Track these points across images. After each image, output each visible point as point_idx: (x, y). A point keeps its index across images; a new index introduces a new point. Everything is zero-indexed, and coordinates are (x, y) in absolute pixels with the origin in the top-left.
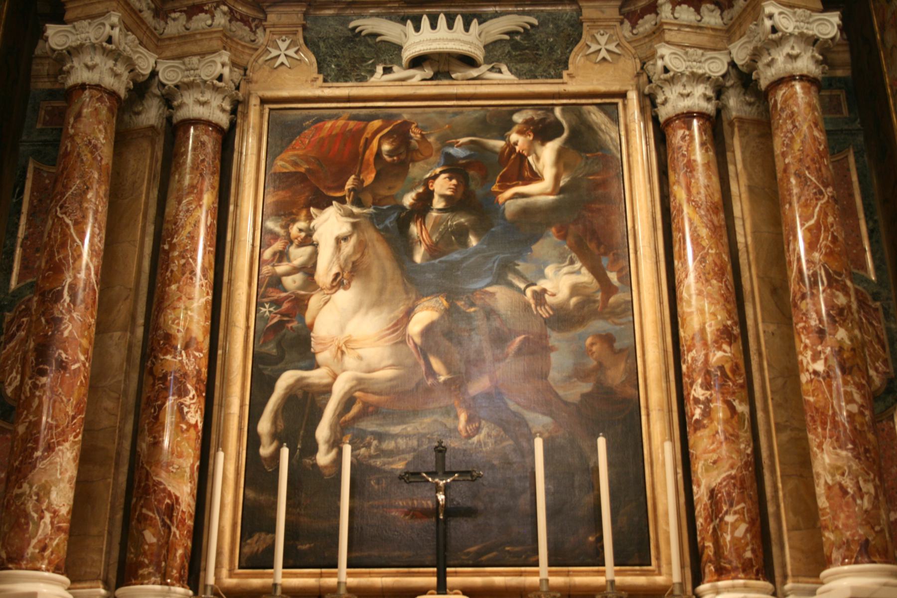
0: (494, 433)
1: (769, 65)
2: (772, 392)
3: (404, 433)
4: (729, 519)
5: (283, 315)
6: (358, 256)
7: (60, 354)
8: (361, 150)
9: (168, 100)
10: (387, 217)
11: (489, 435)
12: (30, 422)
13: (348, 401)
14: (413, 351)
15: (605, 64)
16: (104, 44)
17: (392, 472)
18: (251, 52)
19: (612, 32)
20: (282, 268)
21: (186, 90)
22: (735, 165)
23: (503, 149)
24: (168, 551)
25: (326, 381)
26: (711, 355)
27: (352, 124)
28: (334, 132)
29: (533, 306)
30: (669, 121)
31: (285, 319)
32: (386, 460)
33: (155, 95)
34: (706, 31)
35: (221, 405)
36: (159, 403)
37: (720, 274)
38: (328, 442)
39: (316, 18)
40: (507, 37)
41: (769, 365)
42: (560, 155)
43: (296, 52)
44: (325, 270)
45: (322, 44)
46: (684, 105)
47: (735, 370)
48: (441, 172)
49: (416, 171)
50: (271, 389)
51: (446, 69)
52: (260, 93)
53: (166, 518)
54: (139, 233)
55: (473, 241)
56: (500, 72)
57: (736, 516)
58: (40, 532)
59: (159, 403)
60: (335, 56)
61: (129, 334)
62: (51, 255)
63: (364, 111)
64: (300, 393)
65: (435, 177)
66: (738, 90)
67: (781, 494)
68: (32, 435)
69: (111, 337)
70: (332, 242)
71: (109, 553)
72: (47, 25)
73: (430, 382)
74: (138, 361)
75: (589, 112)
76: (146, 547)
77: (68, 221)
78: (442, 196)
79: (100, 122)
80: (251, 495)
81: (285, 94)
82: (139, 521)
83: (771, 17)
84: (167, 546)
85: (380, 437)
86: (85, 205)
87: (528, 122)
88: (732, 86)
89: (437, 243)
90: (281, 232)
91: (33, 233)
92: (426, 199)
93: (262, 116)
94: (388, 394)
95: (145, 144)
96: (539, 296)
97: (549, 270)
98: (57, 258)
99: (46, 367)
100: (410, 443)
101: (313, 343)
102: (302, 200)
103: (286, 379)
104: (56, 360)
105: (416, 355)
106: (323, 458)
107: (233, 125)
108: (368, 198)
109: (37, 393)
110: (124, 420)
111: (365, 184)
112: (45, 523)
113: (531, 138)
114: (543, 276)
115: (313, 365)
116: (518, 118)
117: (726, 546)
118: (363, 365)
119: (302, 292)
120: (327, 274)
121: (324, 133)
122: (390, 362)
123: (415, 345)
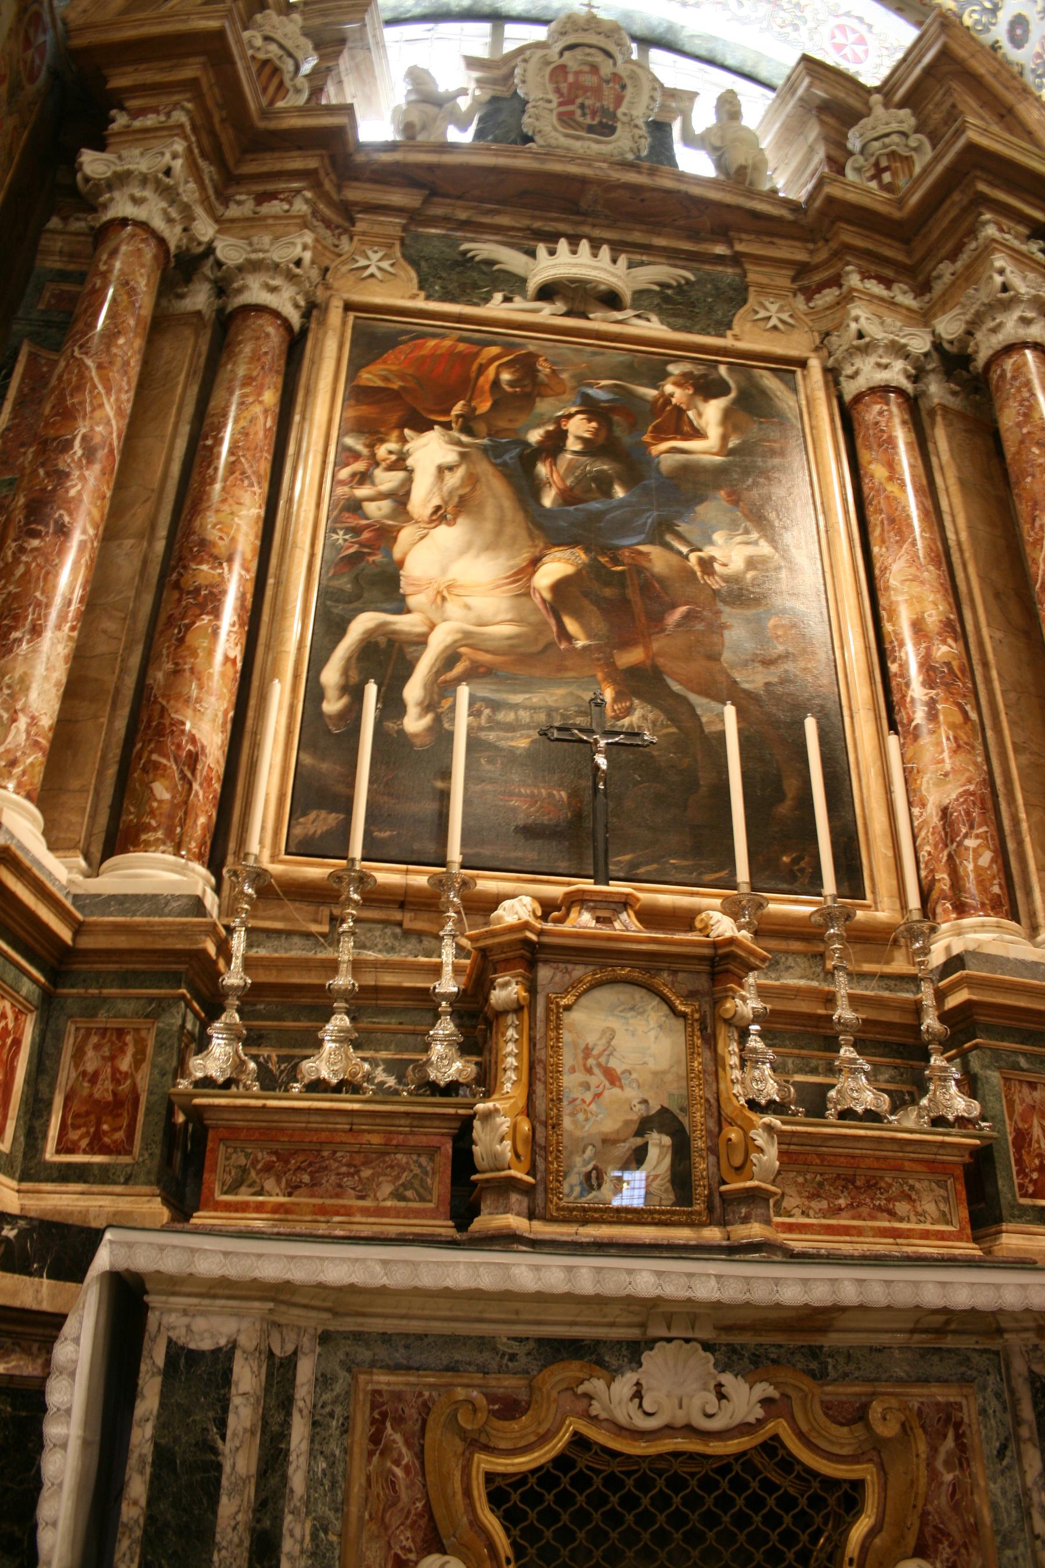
0: (651, 716)
1: (994, 330)
2: (1006, 706)
3: (528, 703)
4: (971, 843)
5: (362, 545)
6: (467, 490)
7: (61, 516)
8: (473, 375)
9: (222, 289)
10: (506, 451)
11: (644, 718)
12: (10, 593)
13: (450, 658)
14: (541, 606)
15: (776, 334)
16: (160, 175)
17: (512, 751)
18: (332, 256)
19: (783, 303)
21: (249, 272)
22: (939, 457)
23: (656, 400)
24: (186, 813)
25: (421, 629)
26: (934, 648)
27: (462, 347)
28: (439, 352)
29: (699, 574)
30: (859, 398)
31: (366, 550)
32: (502, 734)
33: (207, 279)
34: (899, 309)
35: (268, 647)
36: (187, 621)
38: (420, 704)
39: (418, 237)
40: (656, 288)
41: (999, 674)
42: (727, 416)
43: (392, 265)
45: (423, 264)
46: (881, 377)
48: (577, 413)
49: (544, 406)
51: (582, 309)
52: (346, 296)
53: (186, 769)
54: (170, 428)
55: (619, 492)
56: (648, 320)
57: (979, 841)
58: (10, 738)
59: (187, 621)
60: (440, 278)
61: (145, 544)
62: (62, 398)
63: (478, 335)
64: (382, 641)
65: (570, 416)
66: (940, 376)
67: (1024, 826)
68: (10, 610)
69: (119, 546)
70: (432, 471)
71: (93, 817)
72: (83, 150)
73: (563, 646)
74: (154, 580)
75: (761, 376)
76: (155, 804)
77: (89, 362)
78: (579, 438)
79: (143, 266)
80: (307, 760)
81: (378, 300)
82: (145, 770)
83: (1001, 272)
84: (184, 805)
86: (114, 350)
88: (933, 370)
89: (571, 489)
90: (365, 451)
91: (18, 425)
93: (344, 323)
94: (504, 654)
95: (188, 332)
96: (707, 565)
97: (718, 537)
98: (69, 403)
99: (39, 527)
100: (535, 716)
101: (402, 583)
102: (394, 418)
103: (363, 623)
104: (56, 522)
105: (544, 611)
108: (481, 427)
109: (24, 558)
110: (129, 648)
111: (479, 412)
112: (18, 729)
113: (691, 392)
114: (711, 542)
115: (402, 609)
117: (968, 876)
118: (472, 615)
119: (390, 522)
120: (425, 506)
121: (424, 352)
122: (509, 616)
123: (544, 601)
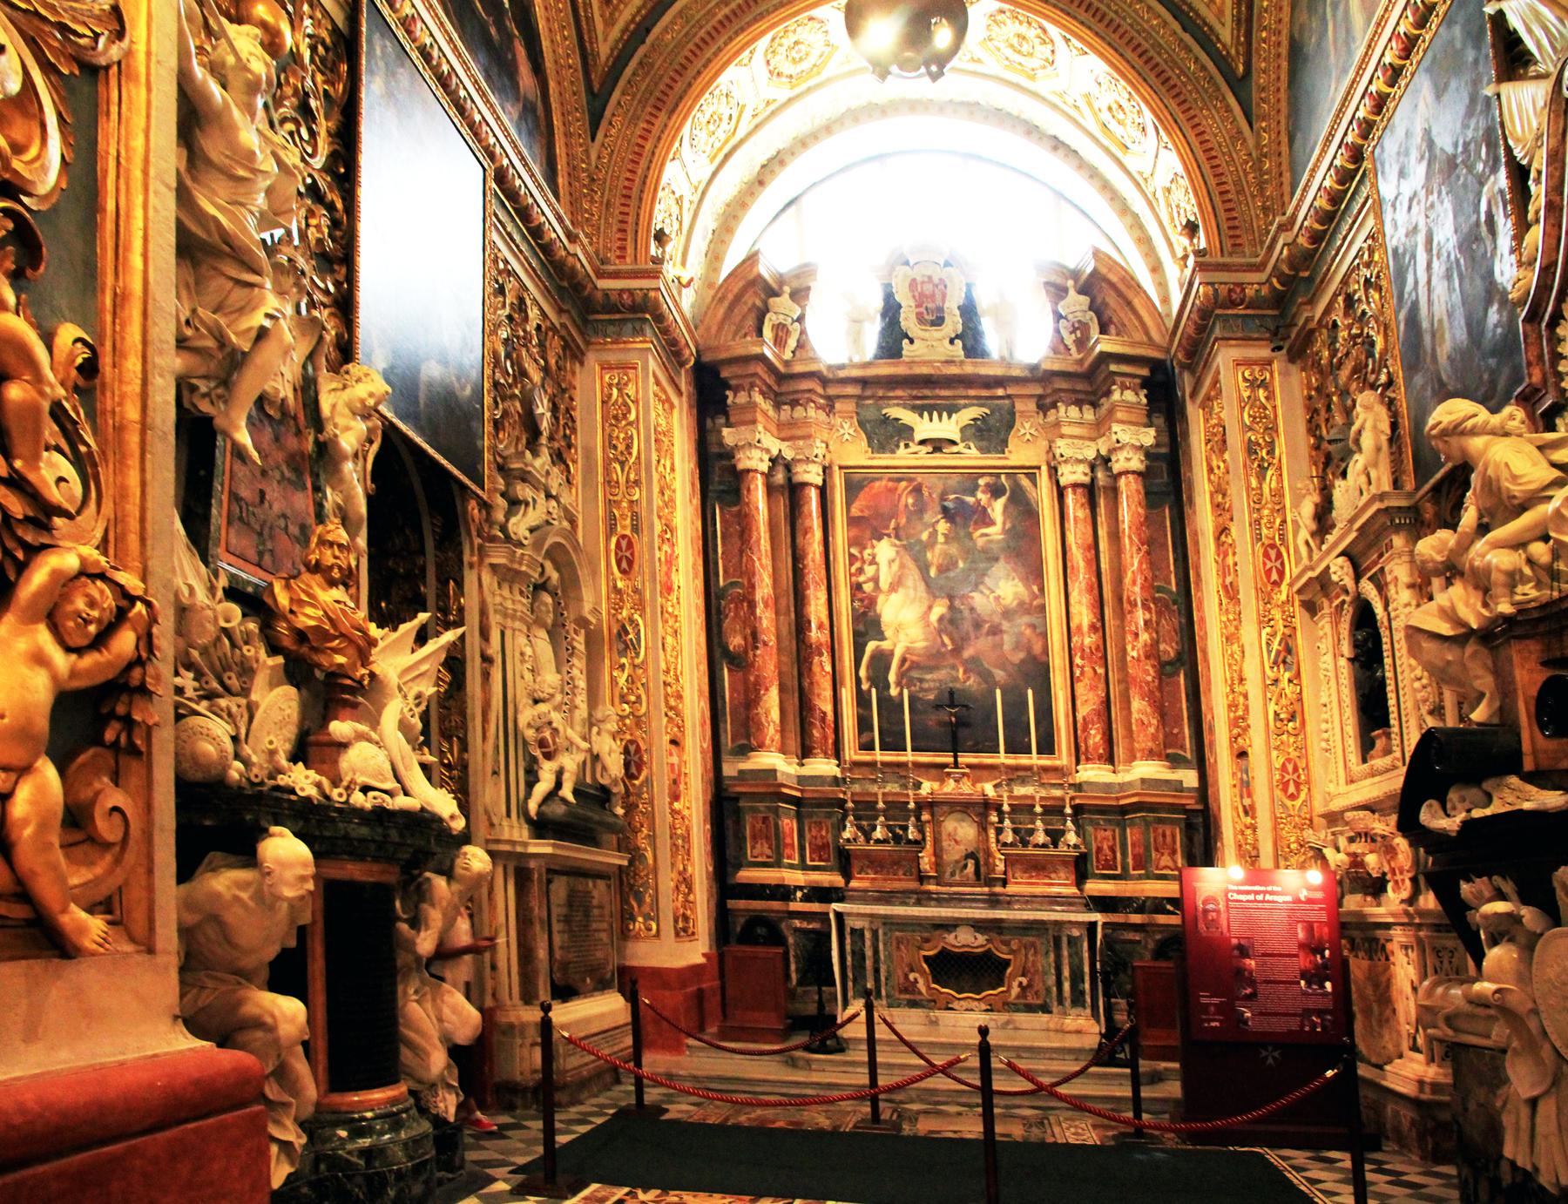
20: (861, 579)
44: (884, 584)
47: (1097, 649)
85: (921, 680)
96: (997, 598)
106: (894, 692)
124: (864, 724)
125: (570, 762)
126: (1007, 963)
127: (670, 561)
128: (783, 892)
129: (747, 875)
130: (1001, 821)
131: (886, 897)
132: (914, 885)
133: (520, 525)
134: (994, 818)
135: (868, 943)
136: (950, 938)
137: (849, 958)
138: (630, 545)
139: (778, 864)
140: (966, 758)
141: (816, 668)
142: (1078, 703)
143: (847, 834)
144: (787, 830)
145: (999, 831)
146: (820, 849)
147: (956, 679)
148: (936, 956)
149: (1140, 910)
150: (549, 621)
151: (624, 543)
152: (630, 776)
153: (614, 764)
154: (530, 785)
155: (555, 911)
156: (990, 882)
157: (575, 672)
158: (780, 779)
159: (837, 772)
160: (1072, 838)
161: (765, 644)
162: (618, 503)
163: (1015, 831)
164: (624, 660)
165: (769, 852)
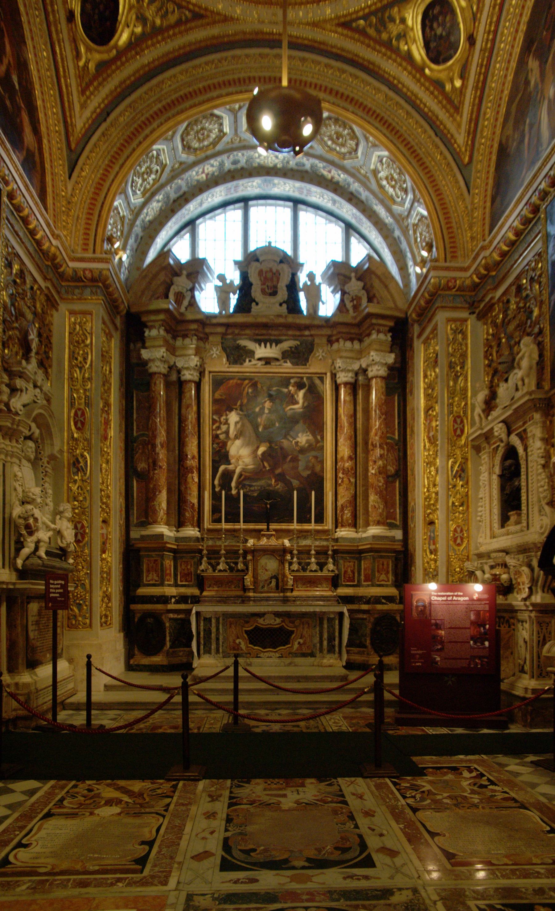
9: (179, 372)
13: (240, 475)
20: (219, 432)
37: (350, 439)
42: (305, 396)
47: (352, 469)
50: (217, 471)
85: (250, 486)
87: (295, 383)
92: (263, 409)
96: (297, 443)
97: (300, 435)
103: (222, 468)
106: (234, 492)
107: (200, 380)
108: (244, 408)
115: (229, 464)
116: (292, 381)
124: (215, 509)
125: (43, 535)
126: (292, 632)
127: (107, 423)
128: (165, 600)
129: (142, 591)
130: (292, 558)
131: (223, 600)
132: (240, 593)
133: (17, 403)
134: (288, 557)
135: (214, 625)
136: (261, 621)
137: (202, 633)
138: (83, 414)
139: (162, 584)
140: (273, 526)
141: (189, 480)
142: (339, 497)
143: (202, 567)
144: (168, 567)
145: (291, 564)
146: (186, 576)
147: (270, 485)
148: (252, 630)
149: (368, 602)
150: (32, 457)
151: (79, 413)
152: (77, 541)
153: (69, 534)
154: (18, 551)
155: (31, 619)
156: (284, 590)
157: (47, 485)
158: (166, 539)
159: (198, 534)
160: (331, 566)
161: (161, 467)
162: (77, 391)
163: (299, 564)
164: (76, 478)
165: (157, 579)
